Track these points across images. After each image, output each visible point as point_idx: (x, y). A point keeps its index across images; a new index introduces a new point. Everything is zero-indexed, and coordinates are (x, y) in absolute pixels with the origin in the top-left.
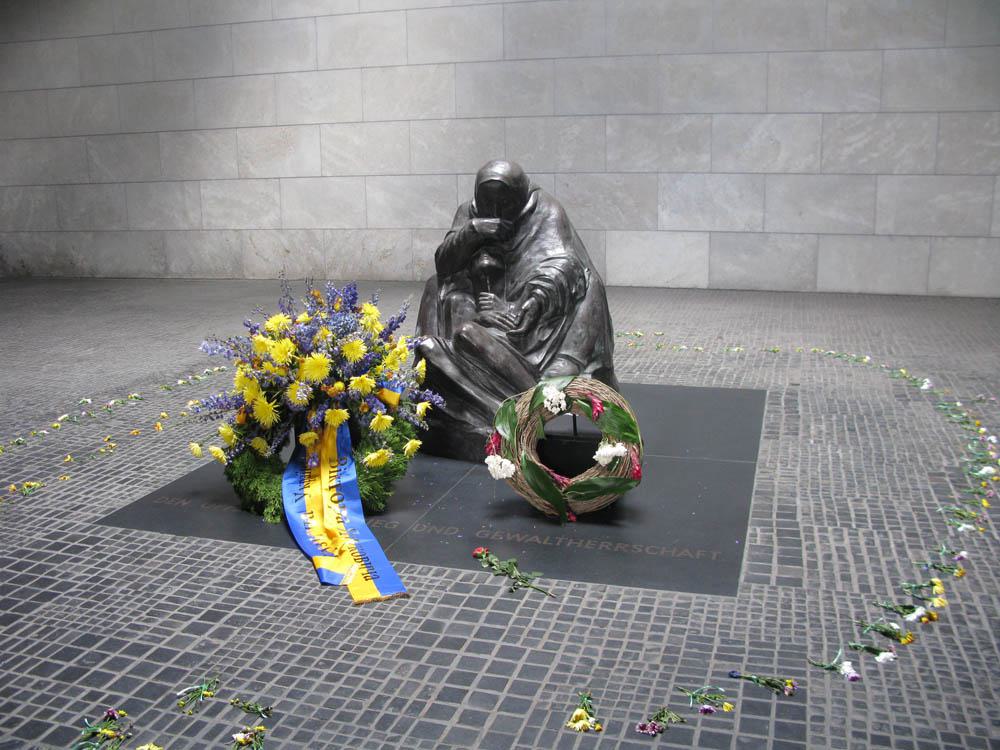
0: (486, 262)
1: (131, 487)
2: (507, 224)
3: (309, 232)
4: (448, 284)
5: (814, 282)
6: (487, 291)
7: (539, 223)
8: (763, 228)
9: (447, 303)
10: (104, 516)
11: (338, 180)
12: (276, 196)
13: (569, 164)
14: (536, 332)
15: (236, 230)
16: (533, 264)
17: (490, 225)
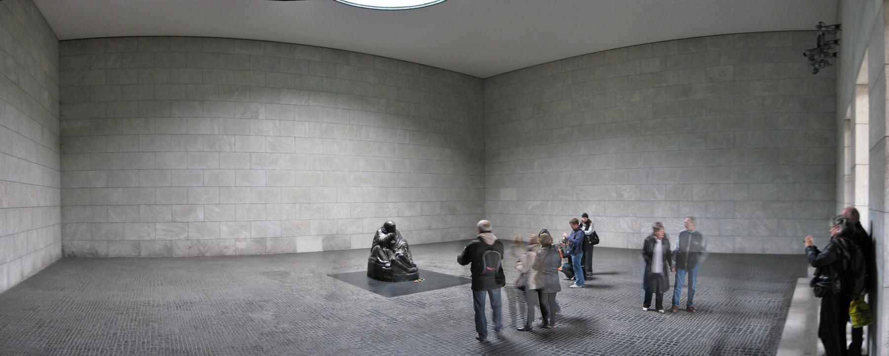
3: (198, 240)
5: (350, 247)
9: (387, 252)
11: (210, 223)
12: (187, 229)
15: (170, 240)
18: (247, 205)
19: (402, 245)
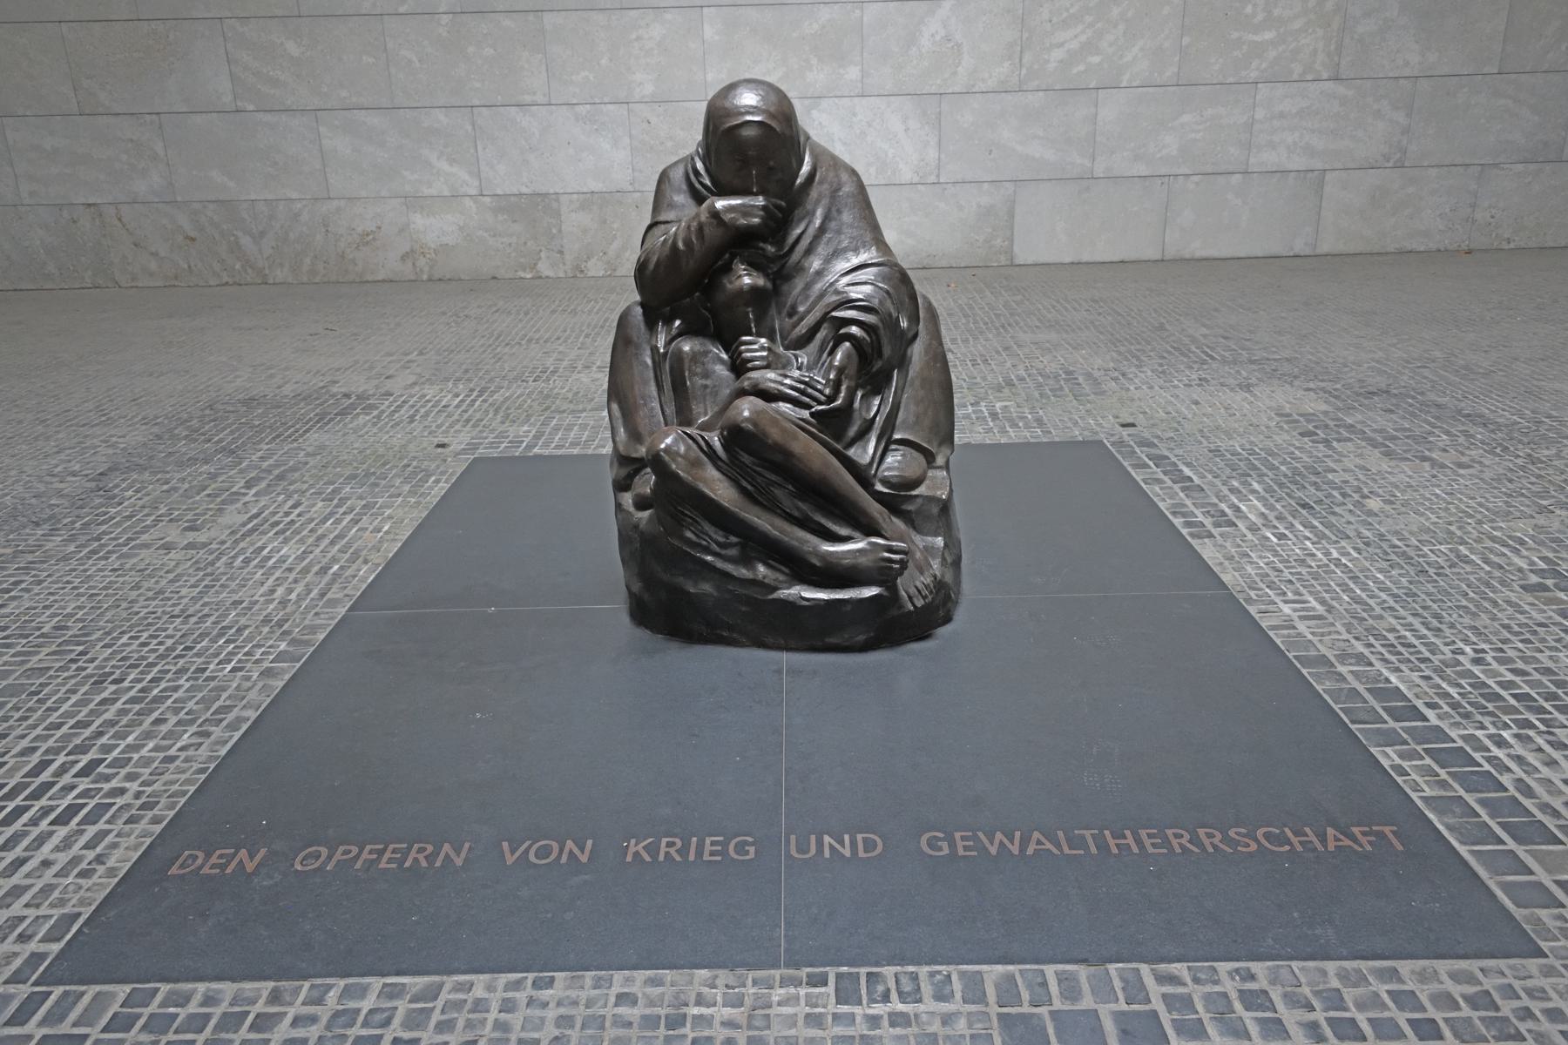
0: (747, 280)
1: (91, 830)
2: (778, 207)
4: (668, 322)
5: (1009, 252)
6: (751, 335)
7: (825, 202)
8: (938, 176)
10: (56, 947)
11: (268, 117)
13: (649, 89)
14: (857, 404)
16: (830, 278)
17: (744, 211)
18: (445, 19)
19: (825, 318)
